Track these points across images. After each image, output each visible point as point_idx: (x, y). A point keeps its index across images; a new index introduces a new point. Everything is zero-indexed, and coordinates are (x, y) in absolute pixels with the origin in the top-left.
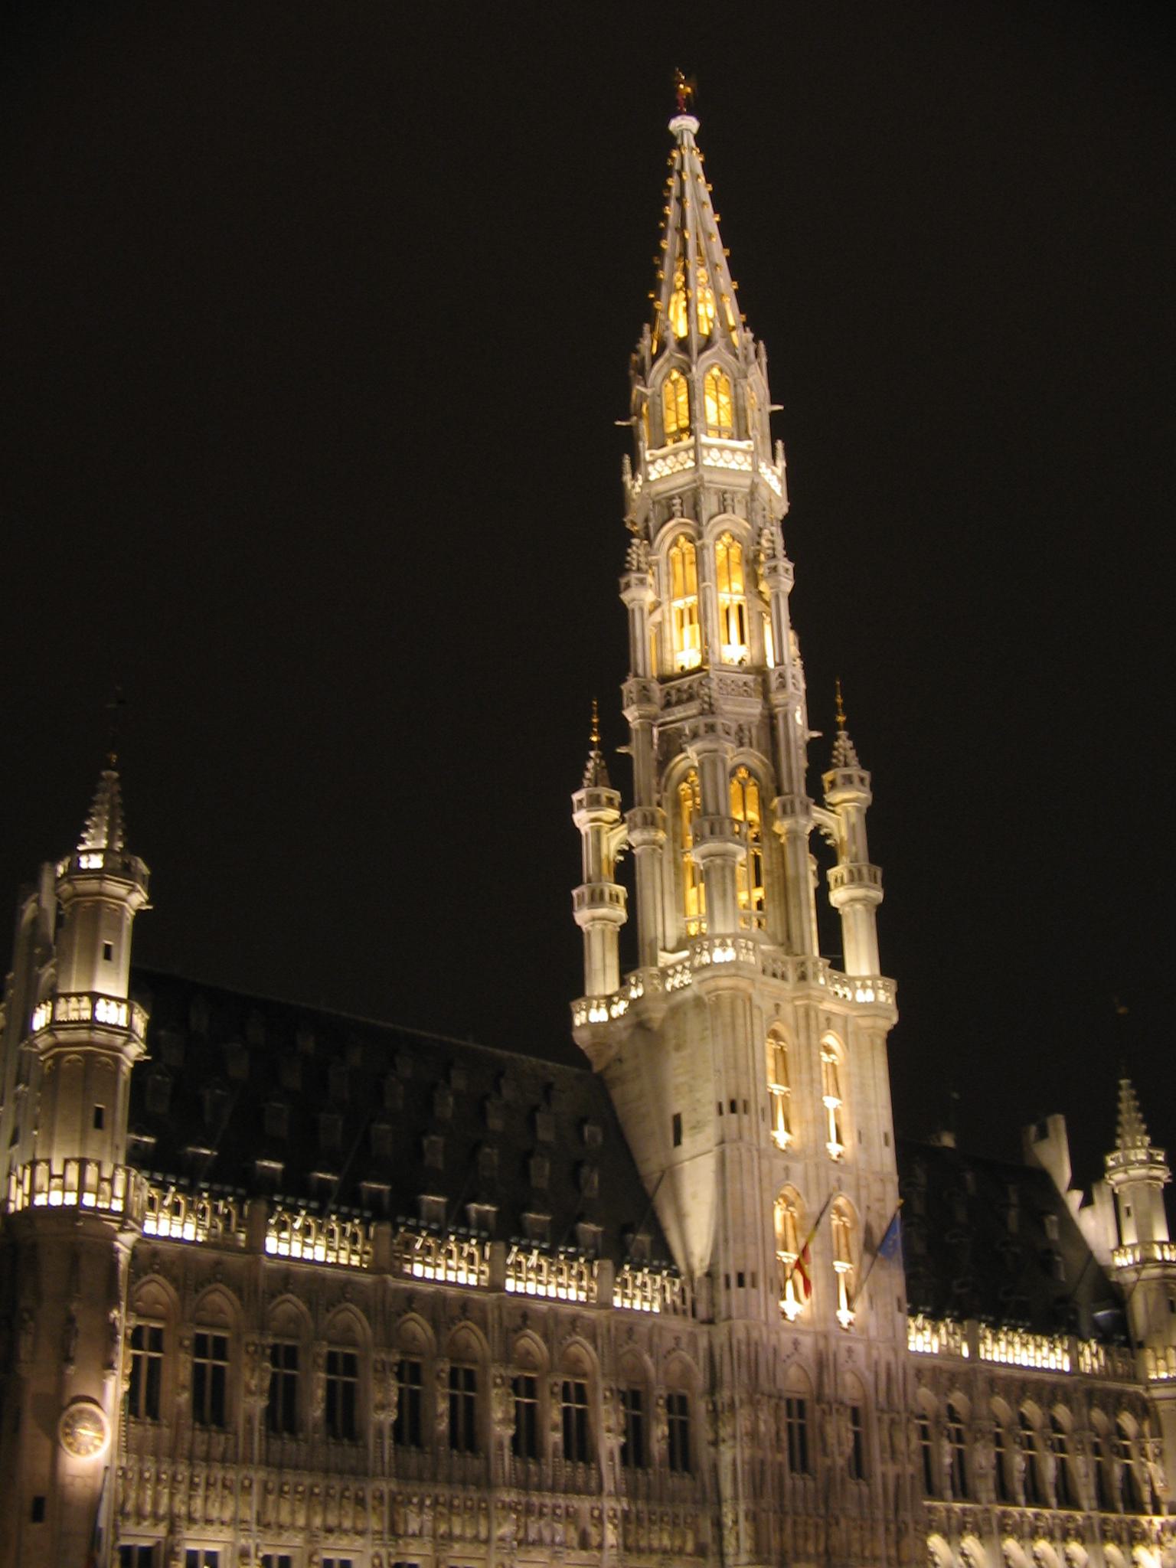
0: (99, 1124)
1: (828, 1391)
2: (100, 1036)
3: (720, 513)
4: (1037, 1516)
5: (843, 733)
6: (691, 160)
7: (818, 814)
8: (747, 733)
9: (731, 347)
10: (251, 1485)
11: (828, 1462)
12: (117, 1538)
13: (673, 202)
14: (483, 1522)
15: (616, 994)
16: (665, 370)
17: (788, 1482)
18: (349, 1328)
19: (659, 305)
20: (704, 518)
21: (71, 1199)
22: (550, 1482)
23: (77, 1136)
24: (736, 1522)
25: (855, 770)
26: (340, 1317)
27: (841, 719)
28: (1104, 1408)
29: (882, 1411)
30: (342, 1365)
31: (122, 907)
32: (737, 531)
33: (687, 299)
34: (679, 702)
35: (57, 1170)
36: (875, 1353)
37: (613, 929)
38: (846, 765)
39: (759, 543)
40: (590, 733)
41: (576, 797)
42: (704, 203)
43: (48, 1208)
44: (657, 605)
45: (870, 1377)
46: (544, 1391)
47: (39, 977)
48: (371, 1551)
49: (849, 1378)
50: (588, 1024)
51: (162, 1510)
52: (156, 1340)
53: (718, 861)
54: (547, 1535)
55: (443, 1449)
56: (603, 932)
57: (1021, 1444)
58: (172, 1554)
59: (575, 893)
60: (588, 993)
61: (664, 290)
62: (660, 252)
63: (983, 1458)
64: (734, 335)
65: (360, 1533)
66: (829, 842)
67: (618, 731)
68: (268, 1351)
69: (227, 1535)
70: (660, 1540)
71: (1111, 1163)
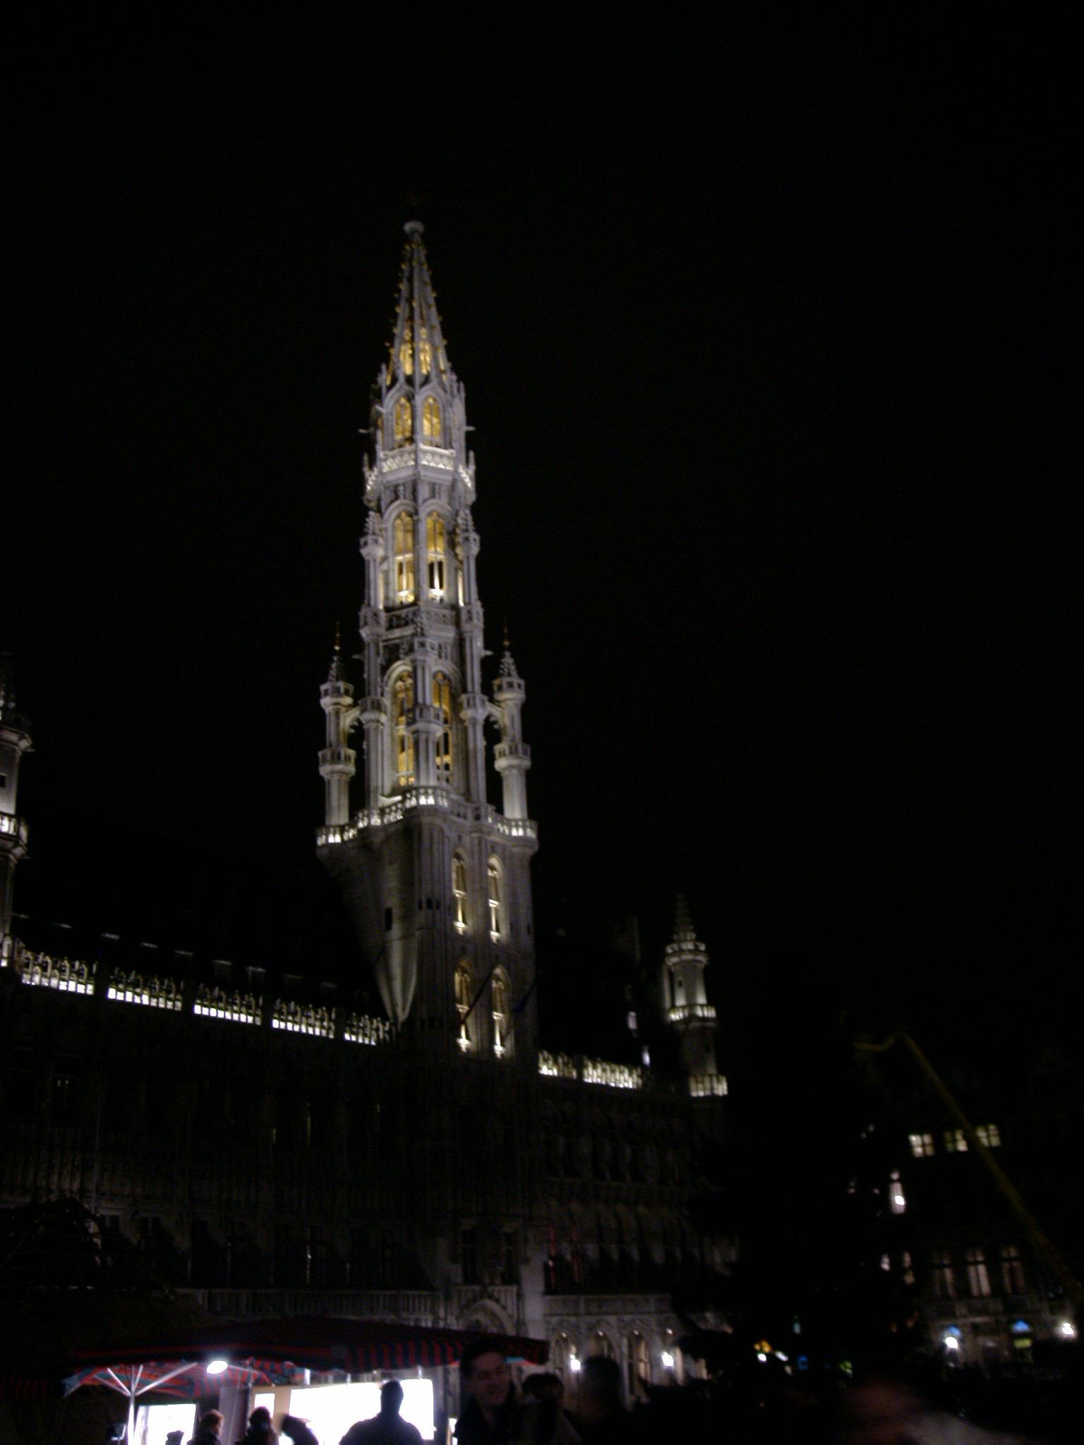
5: (507, 654)
7: (491, 708)
8: (444, 650)
9: (442, 384)
13: (405, 281)
15: (348, 825)
16: (396, 397)
19: (392, 351)
20: (420, 499)
25: (516, 680)
27: (507, 643)
32: (441, 511)
33: (413, 349)
34: (399, 626)
37: (345, 778)
38: (509, 675)
39: (456, 520)
41: (323, 688)
42: (425, 283)
56: (339, 780)
59: (320, 754)
60: (327, 823)
61: (397, 341)
62: (395, 315)
64: (444, 377)
66: (496, 727)
71: (670, 951)
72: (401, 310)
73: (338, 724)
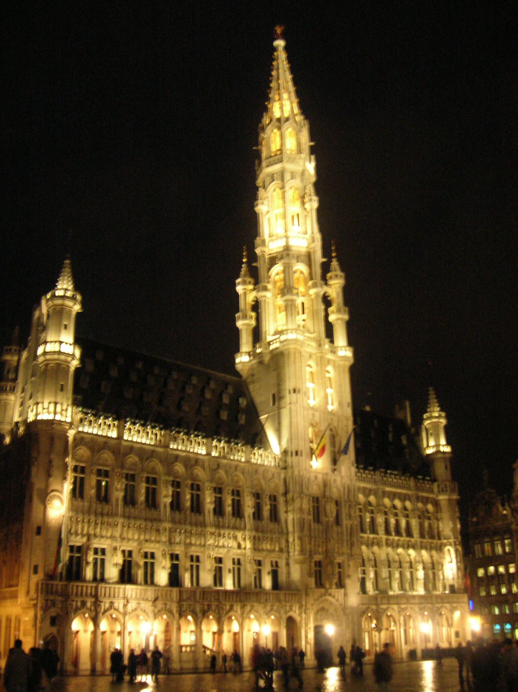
0: (62, 390)
1: (327, 494)
2: (63, 357)
3: (291, 180)
4: (399, 540)
6: (282, 56)
7: (325, 289)
9: (295, 121)
10: (117, 525)
11: (327, 519)
12: (68, 542)
14: (203, 539)
17: (313, 526)
18: (154, 468)
20: (286, 180)
21: (51, 417)
22: (227, 525)
23: (53, 394)
24: (294, 540)
25: (339, 273)
26: (150, 464)
28: (422, 502)
29: (346, 501)
30: (152, 481)
31: (71, 310)
35: (46, 405)
36: (344, 481)
38: (335, 271)
40: (242, 258)
43: (42, 421)
44: (268, 212)
45: (342, 489)
46: (225, 492)
47: (40, 338)
48: (162, 549)
49: (334, 490)
50: (241, 362)
51: (85, 532)
52: (83, 470)
53: (290, 303)
54: (226, 544)
55: (188, 512)
57: (393, 514)
58: (88, 548)
60: (241, 351)
62: (270, 88)
63: (380, 520)
65: (158, 542)
66: (329, 298)
67: (253, 257)
68: (124, 475)
69: (109, 541)
70: (266, 546)
72: (273, 85)
73: (245, 300)
